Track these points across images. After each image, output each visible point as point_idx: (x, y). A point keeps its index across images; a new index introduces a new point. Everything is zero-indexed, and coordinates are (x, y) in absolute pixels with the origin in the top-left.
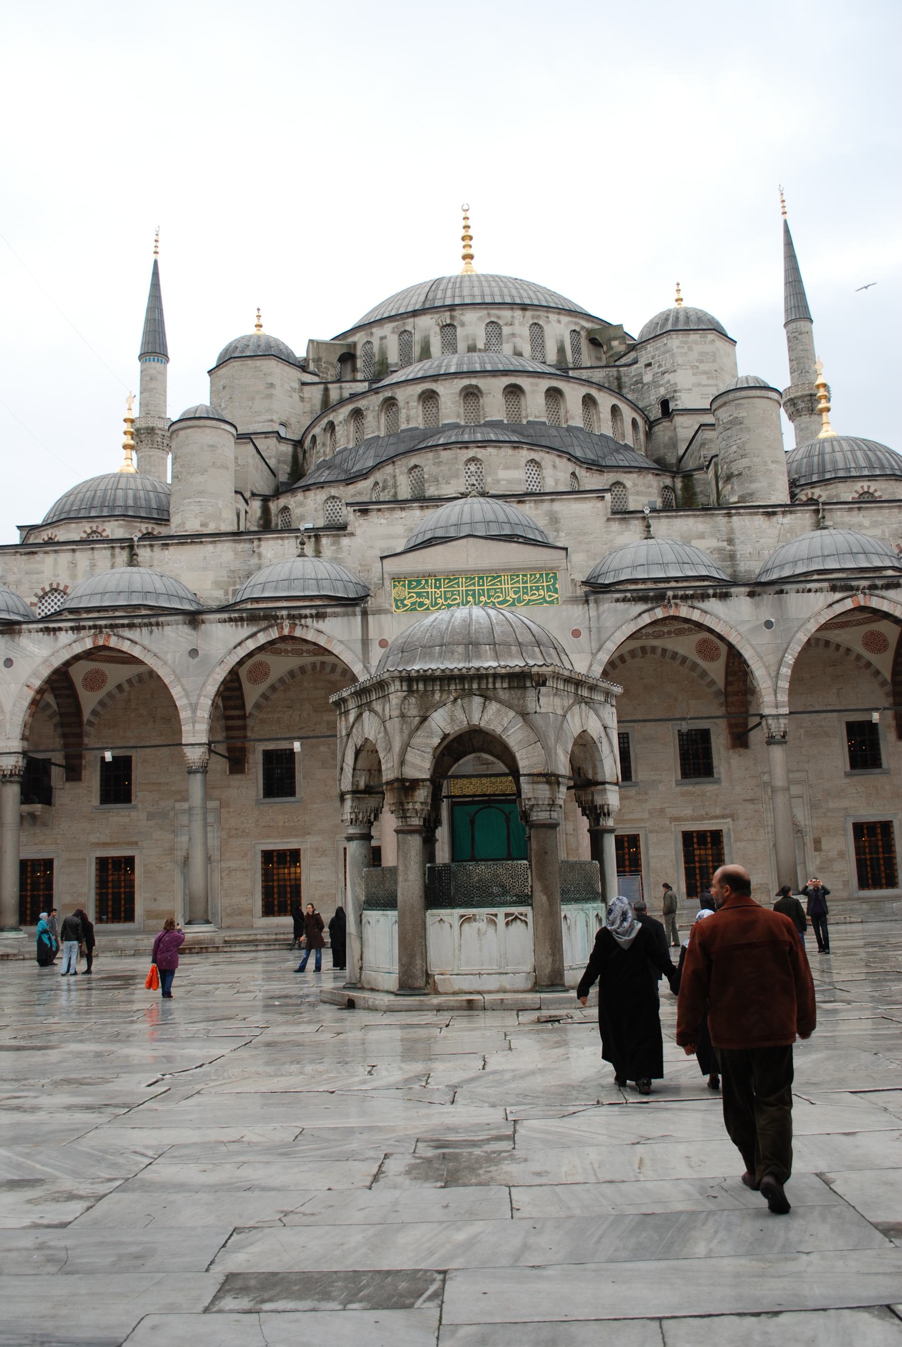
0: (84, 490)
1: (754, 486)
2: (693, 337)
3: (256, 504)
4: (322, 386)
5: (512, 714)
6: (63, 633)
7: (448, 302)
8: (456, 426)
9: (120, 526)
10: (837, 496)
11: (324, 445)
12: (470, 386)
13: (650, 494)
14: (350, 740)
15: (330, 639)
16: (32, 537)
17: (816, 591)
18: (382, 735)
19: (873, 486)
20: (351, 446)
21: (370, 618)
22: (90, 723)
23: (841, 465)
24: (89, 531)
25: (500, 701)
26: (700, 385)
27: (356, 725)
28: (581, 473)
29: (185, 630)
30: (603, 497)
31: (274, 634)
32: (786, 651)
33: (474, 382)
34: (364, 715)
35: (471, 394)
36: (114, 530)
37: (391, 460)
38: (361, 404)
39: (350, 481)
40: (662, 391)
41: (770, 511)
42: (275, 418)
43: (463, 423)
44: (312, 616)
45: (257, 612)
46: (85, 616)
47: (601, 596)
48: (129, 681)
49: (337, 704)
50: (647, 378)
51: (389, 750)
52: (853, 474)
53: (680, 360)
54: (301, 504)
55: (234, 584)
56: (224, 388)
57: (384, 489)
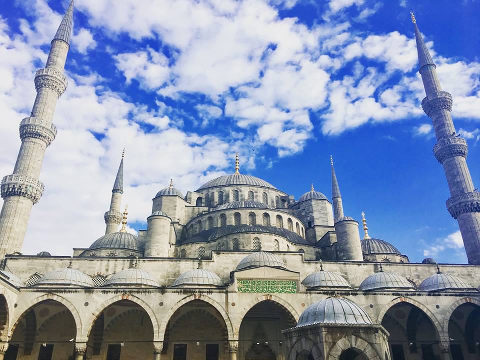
0: (109, 237)
1: (352, 254)
2: (319, 201)
3: (173, 247)
4: (192, 207)
5: (366, 343)
6: (111, 293)
7: (235, 183)
8: (246, 226)
9: (122, 252)
10: (376, 260)
11: (196, 228)
12: (252, 212)
13: (311, 254)
14: (293, 350)
15: (214, 301)
16: (86, 254)
17: (387, 295)
18: (314, 350)
19: (388, 257)
20: (207, 230)
21: (229, 294)
22: (106, 330)
23: (376, 248)
24: (110, 253)
25: (361, 338)
26: (321, 217)
27: (297, 343)
28: (290, 245)
29: (159, 294)
30: (301, 255)
31: (192, 298)
32: (378, 316)
33: (253, 211)
34: (302, 340)
35: (252, 215)
36: (119, 253)
37: (226, 236)
38: (213, 215)
39: (208, 242)
40: (309, 218)
41: (359, 264)
42: (176, 217)
43: (248, 225)
44: (207, 292)
45: (187, 290)
46: (119, 287)
47: (312, 291)
48: (124, 313)
49: (285, 334)
50: (303, 214)
51: (321, 354)
52: (380, 252)
53: (314, 208)
54: (190, 249)
55: (169, 277)
56: (159, 205)
57: (222, 246)
